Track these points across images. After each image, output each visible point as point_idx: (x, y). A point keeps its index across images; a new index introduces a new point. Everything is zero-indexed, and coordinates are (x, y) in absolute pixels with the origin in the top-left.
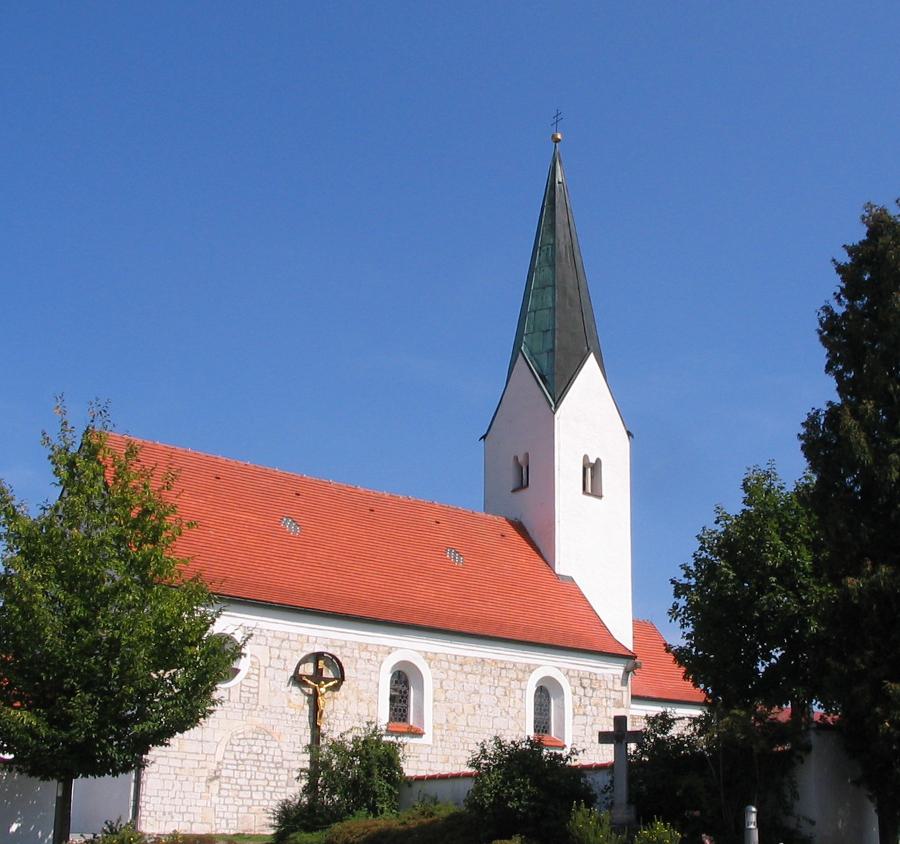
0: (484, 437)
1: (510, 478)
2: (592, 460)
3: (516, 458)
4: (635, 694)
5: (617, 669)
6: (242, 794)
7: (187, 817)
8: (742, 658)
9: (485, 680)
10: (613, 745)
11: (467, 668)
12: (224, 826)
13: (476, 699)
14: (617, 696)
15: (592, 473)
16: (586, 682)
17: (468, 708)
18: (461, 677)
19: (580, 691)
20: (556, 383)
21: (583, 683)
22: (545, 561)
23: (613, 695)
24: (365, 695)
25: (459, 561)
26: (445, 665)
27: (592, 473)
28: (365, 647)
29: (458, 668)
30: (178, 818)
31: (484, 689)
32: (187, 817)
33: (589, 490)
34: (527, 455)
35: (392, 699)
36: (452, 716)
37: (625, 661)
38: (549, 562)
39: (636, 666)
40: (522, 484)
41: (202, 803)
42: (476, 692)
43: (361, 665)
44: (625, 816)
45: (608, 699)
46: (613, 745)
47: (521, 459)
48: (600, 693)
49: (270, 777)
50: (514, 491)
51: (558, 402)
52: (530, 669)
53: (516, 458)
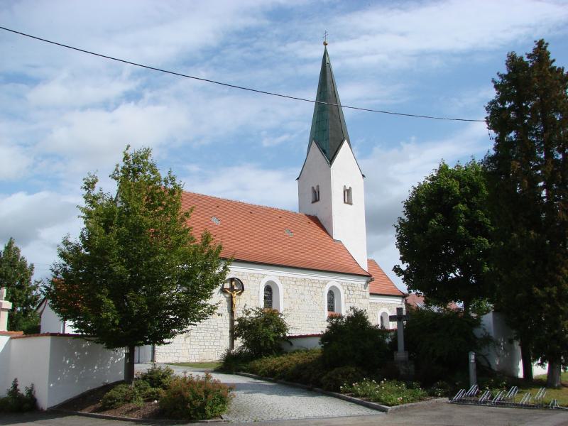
0: (298, 179)
1: (310, 197)
2: (348, 188)
3: (313, 188)
4: (372, 292)
5: (362, 282)
6: (201, 343)
7: (176, 355)
8: (470, 268)
9: (306, 288)
10: (396, 322)
11: (298, 283)
12: (193, 357)
13: (302, 297)
14: (364, 293)
15: (347, 193)
16: (350, 288)
17: (299, 301)
18: (296, 287)
19: (348, 292)
20: (330, 154)
21: (350, 289)
22: (328, 234)
23: (362, 293)
24: (253, 297)
25: (291, 235)
26: (288, 282)
27: (347, 193)
28: (253, 275)
29: (293, 283)
30: (172, 355)
31: (306, 293)
32: (176, 355)
33: (347, 201)
34: (318, 186)
35: (265, 298)
36: (292, 305)
37: (366, 278)
38: (330, 236)
39: (372, 280)
40: (316, 199)
41: (183, 348)
42: (302, 294)
43: (251, 283)
44: (404, 356)
45: (360, 295)
46: (396, 322)
47: (315, 188)
48: (356, 293)
49: (213, 335)
50: (313, 202)
51: (331, 161)
52: (325, 283)
53: (313, 188)
